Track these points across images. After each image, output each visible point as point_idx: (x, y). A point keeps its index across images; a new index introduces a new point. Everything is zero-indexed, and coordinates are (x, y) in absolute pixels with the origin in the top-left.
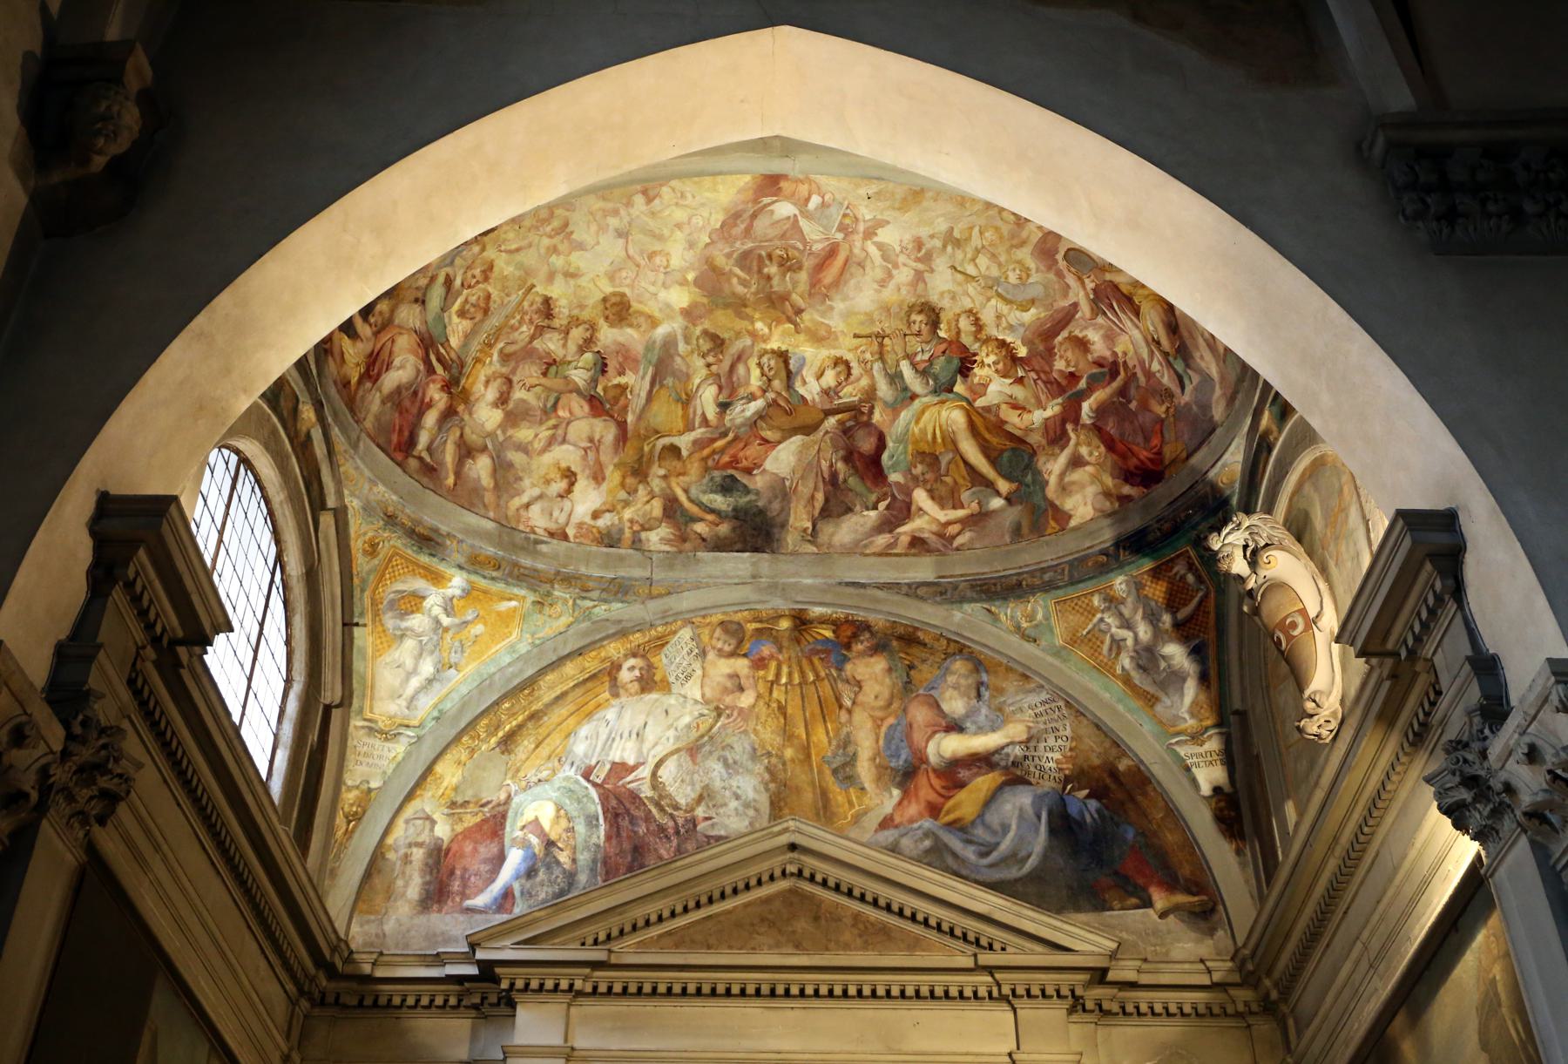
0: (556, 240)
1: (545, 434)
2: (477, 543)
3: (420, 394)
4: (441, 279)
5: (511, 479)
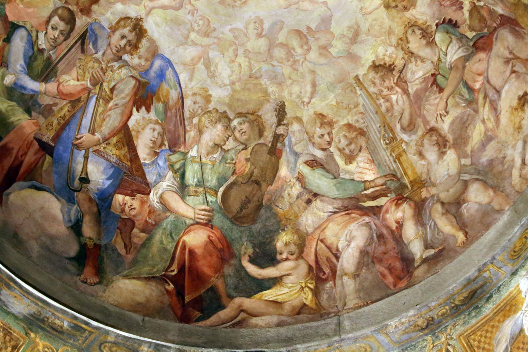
0: (314, 46)
1: (485, 112)
2: (504, 243)
3: (385, 232)
4: (305, 170)
5: (499, 168)
